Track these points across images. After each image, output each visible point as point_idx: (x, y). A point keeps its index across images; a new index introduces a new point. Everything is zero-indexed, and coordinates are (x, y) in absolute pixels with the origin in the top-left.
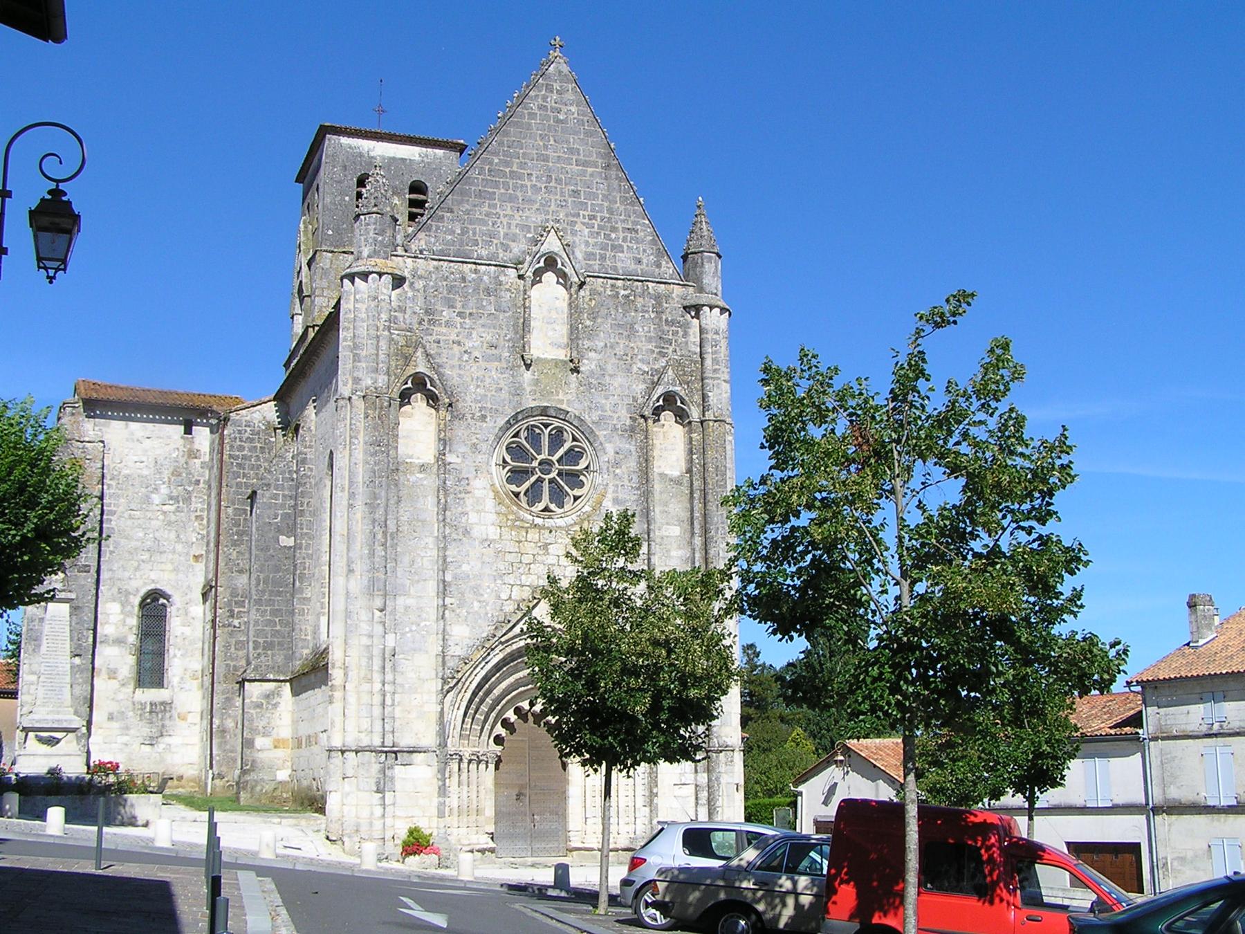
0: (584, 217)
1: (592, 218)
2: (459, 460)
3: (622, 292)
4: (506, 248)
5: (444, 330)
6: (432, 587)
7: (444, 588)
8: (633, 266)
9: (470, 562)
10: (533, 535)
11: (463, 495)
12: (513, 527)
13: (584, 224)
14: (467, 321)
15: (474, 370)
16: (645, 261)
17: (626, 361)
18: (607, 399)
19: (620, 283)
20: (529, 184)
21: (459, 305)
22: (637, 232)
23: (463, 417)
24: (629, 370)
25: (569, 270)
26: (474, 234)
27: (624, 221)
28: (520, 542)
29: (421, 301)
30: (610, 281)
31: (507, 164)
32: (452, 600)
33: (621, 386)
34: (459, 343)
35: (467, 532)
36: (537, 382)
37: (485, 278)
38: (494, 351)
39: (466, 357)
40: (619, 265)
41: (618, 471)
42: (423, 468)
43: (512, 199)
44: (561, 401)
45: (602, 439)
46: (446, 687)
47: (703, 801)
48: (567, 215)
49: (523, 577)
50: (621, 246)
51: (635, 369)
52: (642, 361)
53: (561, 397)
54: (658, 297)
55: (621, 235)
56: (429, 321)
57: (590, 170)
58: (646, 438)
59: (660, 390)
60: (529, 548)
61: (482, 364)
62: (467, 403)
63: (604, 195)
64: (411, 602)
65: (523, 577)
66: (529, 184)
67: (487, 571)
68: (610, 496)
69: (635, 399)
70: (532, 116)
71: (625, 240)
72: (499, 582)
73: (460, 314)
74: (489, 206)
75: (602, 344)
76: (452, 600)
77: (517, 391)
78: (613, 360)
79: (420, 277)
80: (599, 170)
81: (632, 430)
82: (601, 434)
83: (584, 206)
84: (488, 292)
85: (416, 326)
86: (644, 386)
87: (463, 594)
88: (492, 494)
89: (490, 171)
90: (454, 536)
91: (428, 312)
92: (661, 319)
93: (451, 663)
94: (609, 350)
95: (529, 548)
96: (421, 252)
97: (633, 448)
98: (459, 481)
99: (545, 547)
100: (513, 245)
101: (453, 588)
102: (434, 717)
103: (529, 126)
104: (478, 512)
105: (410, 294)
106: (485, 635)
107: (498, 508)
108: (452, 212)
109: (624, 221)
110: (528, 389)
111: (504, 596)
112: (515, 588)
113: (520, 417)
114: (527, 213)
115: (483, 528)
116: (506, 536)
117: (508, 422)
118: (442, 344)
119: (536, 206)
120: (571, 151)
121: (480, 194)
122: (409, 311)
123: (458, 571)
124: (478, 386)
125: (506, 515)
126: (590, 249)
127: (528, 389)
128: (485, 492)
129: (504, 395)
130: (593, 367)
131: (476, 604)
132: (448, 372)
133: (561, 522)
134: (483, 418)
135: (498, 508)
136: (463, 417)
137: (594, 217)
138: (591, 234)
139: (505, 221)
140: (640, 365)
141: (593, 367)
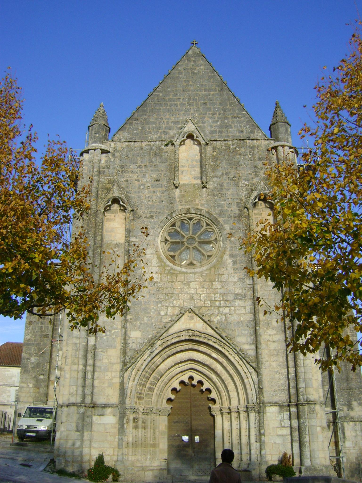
0: (209, 114)
1: (213, 114)
4: (166, 133)
5: (130, 175)
8: (238, 134)
10: (181, 277)
12: (168, 274)
13: (209, 117)
14: (143, 169)
15: (146, 192)
16: (245, 131)
17: (235, 180)
18: (224, 200)
19: (230, 142)
20: (178, 103)
21: (139, 162)
22: (240, 118)
23: (139, 217)
24: (237, 186)
25: (200, 139)
26: (149, 128)
27: (232, 114)
28: (172, 282)
29: (118, 162)
30: (225, 142)
31: (166, 95)
32: (131, 317)
33: (232, 194)
34: (138, 180)
36: (183, 196)
37: (154, 148)
38: (158, 183)
39: (142, 187)
40: (230, 134)
41: (232, 239)
42: (117, 245)
43: (169, 111)
44: (197, 205)
45: (222, 222)
46: (125, 368)
47: (296, 438)
48: (200, 114)
49: (175, 302)
50: (231, 125)
51: (240, 184)
52: (245, 180)
53: (197, 202)
54: (253, 147)
55: (231, 120)
56: (122, 171)
57: (212, 93)
58: (249, 220)
59: (255, 193)
61: (152, 189)
62: (142, 211)
63: (220, 103)
65: (175, 302)
66: (178, 103)
67: (153, 299)
68: (228, 253)
69: (241, 200)
70: (180, 73)
71: (233, 122)
72: (160, 305)
73: (140, 166)
74: (157, 115)
75: (221, 173)
76: (131, 317)
77: (171, 202)
78: (227, 181)
79: (119, 151)
80: (218, 92)
81: (240, 216)
82: (221, 220)
83: (209, 109)
84: (155, 154)
85: (115, 174)
86: (247, 192)
87: (137, 313)
88: (156, 257)
89: (158, 99)
91: (122, 166)
92: (255, 158)
93: (129, 354)
94: (225, 176)
95: (178, 285)
96: (120, 140)
97: (241, 226)
99: (188, 284)
100: (170, 131)
102: (118, 386)
103: (178, 78)
105: (112, 159)
106: (150, 336)
107: (160, 264)
108: (137, 120)
109: (232, 114)
110: (178, 200)
112: (170, 309)
113: (174, 215)
114: (178, 116)
116: (164, 279)
117: (167, 218)
118: (129, 182)
119: (183, 112)
120: (202, 85)
121: (152, 110)
122: (111, 168)
124: (149, 201)
126: (213, 129)
127: (178, 200)
128: (152, 256)
129: (164, 204)
130: (215, 185)
131: (145, 318)
132: (132, 195)
133: (199, 270)
134: (152, 217)
135: (160, 264)
136: (139, 217)
137: (215, 114)
138: (214, 122)
139: (166, 121)
140: (243, 182)
141: (215, 185)
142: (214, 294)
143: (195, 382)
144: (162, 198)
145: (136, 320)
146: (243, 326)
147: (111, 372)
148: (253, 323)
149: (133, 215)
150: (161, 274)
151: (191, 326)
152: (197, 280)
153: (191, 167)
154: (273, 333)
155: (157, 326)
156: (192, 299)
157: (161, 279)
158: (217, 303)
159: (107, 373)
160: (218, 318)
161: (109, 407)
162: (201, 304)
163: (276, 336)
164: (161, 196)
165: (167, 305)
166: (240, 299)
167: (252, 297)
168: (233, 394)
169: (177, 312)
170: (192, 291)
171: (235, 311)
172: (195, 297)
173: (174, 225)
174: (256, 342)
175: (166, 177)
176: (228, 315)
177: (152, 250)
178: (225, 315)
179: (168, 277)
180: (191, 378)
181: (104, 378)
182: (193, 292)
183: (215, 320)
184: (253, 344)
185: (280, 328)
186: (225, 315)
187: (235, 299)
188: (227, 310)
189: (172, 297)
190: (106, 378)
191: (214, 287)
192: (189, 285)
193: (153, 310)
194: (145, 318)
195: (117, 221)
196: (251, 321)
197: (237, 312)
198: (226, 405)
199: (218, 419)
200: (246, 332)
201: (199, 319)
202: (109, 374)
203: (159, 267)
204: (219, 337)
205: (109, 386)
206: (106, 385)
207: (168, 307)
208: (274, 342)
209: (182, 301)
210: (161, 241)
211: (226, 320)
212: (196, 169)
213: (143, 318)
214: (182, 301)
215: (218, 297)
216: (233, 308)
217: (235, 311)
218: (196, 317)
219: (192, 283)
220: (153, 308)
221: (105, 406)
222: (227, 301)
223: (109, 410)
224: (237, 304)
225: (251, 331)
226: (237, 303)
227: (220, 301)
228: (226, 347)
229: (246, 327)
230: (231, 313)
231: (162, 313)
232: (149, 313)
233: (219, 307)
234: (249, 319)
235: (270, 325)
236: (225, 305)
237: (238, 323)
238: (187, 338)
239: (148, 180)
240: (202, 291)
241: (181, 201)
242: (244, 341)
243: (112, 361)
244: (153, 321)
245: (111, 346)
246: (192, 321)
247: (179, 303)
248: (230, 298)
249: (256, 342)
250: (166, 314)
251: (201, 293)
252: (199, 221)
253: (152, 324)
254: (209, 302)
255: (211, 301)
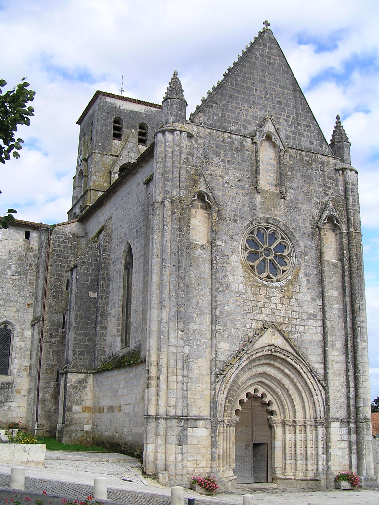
2: (223, 244)
3: (305, 158)
6: (208, 318)
7: (214, 320)
9: (230, 305)
11: (225, 265)
16: (315, 143)
28: (256, 294)
35: (228, 287)
49: (258, 315)
60: (261, 298)
64: (196, 327)
65: (258, 315)
77: (253, 208)
90: (221, 289)
98: (223, 256)
99: (270, 298)
101: (220, 320)
104: (233, 275)
107: (244, 274)
111: (248, 326)
112: (254, 322)
113: (254, 222)
115: (237, 285)
123: (223, 310)
125: (249, 278)
131: (233, 330)
134: (236, 221)
135: (244, 274)
142: (292, 312)
143: (259, 395)
144: (245, 201)
145: (224, 331)
146: (314, 346)
147: (202, 383)
148: (322, 343)
149: (219, 215)
150: (246, 285)
151: (273, 342)
152: (277, 295)
153: (266, 171)
154: (336, 354)
155: (244, 339)
156: (273, 314)
157: (246, 291)
158: (294, 321)
159: (199, 385)
160: (295, 335)
161: (201, 420)
162: (281, 320)
163: (339, 357)
164: (244, 199)
165: (252, 318)
166: (313, 319)
167: (322, 318)
168: (299, 408)
169: (260, 326)
170: (273, 306)
171: (308, 330)
172: (276, 312)
173: (252, 233)
174: (325, 361)
175: (248, 178)
176: (302, 334)
177: (237, 258)
178: (300, 333)
179: (253, 289)
180: (256, 390)
181: (196, 389)
182: (274, 307)
183: (292, 337)
184: (322, 363)
185: (342, 350)
186: (300, 333)
187: (308, 318)
188: (302, 329)
189: (256, 310)
190: (197, 390)
191: (292, 304)
192: (271, 300)
193: (239, 322)
194: (233, 330)
195: (198, 218)
196: (321, 341)
197: (310, 331)
198: (289, 419)
199: (278, 431)
200: (316, 352)
201: (279, 335)
202: (200, 385)
203: (244, 277)
204: (294, 353)
205: (200, 398)
206: (198, 396)
207: (252, 320)
208: (337, 362)
209: (264, 316)
210: (242, 249)
211: (301, 338)
212: (271, 175)
213: (231, 330)
214: (264, 316)
215: (295, 315)
216: (306, 327)
217: (308, 330)
218: (277, 334)
219: (273, 298)
220: (240, 320)
221: (197, 419)
222: (302, 320)
223: (201, 423)
224: (309, 323)
225: (321, 350)
226: (310, 322)
227: (296, 319)
228: (301, 365)
229: (316, 347)
230: (306, 332)
231: (248, 326)
232: (236, 325)
233: (295, 325)
234: (319, 339)
235: (335, 347)
236: (300, 323)
237: (311, 342)
238: (269, 353)
239: (232, 178)
240: (281, 307)
241: (262, 209)
242: (314, 359)
243: (203, 372)
244: (239, 333)
245: (202, 356)
246: (274, 337)
247: (262, 317)
248: (305, 316)
249: (325, 361)
250: (251, 327)
251: (281, 309)
252: (274, 233)
253: (239, 336)
254: (287, 319)
255: (289, 318)
